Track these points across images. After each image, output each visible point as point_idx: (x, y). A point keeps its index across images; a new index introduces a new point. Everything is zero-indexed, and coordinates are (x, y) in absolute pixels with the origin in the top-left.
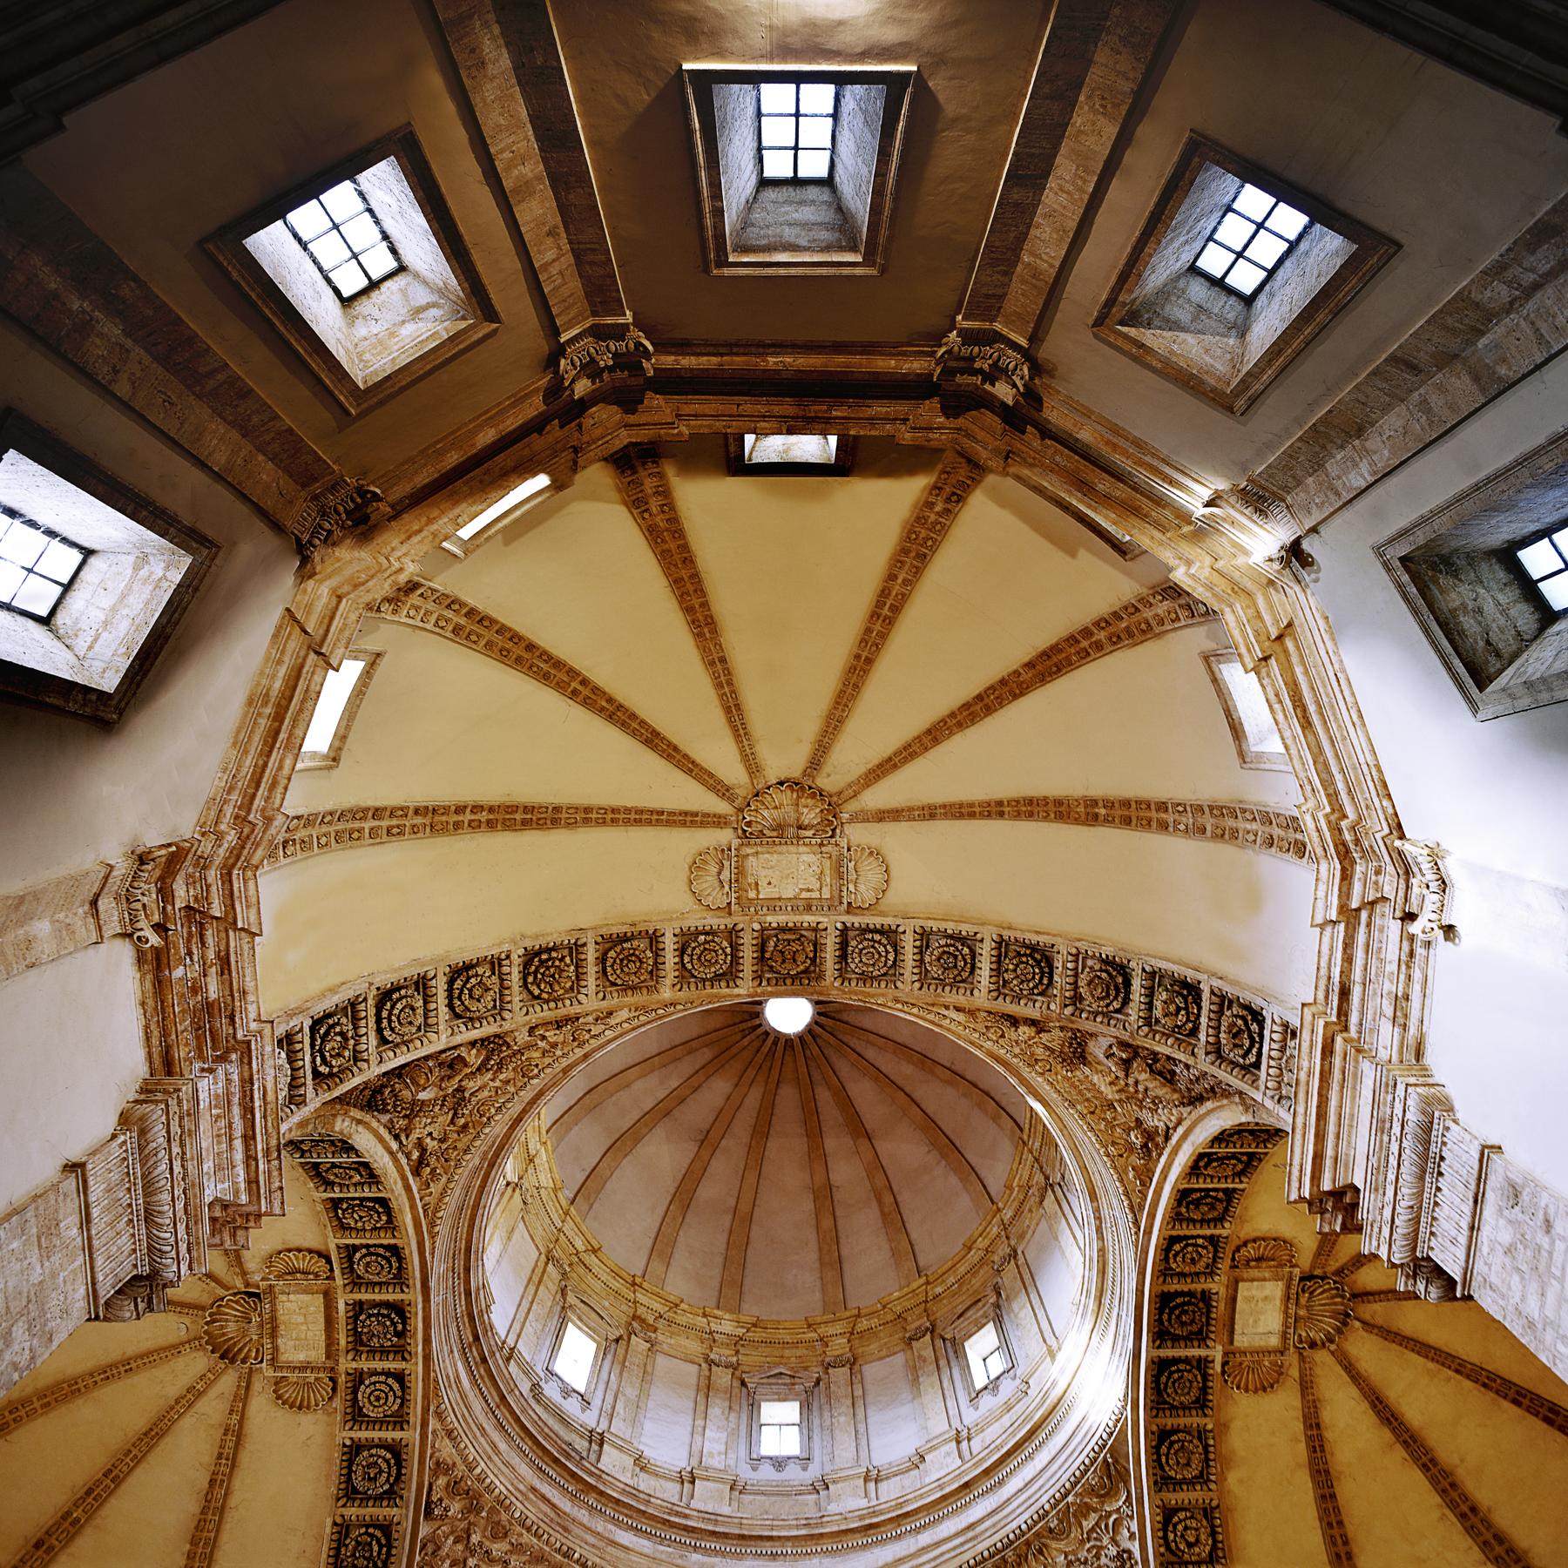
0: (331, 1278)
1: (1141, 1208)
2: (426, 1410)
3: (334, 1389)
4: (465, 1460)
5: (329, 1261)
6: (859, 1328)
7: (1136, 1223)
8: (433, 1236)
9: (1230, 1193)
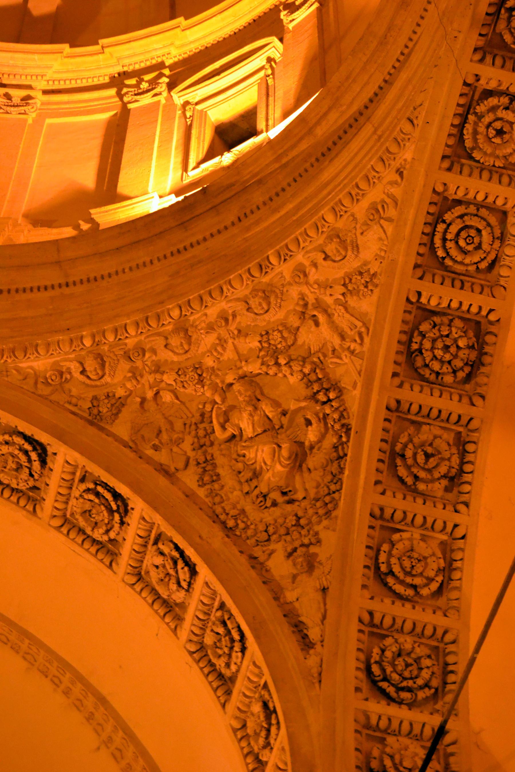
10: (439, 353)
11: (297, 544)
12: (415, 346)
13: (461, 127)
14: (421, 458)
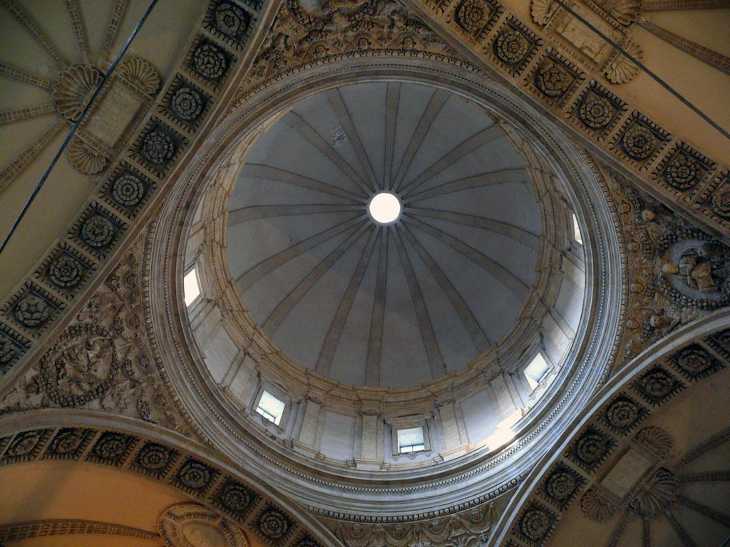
0: (154, 96)
1: (617, 370)
3: (105, 168)
4: (145, 266)
5: (161, 84)
6: (332, 393)
7: (607, 378)
9: (677, 385)
10: (110, 446)
11: (40, 385)
14: (68, 441)
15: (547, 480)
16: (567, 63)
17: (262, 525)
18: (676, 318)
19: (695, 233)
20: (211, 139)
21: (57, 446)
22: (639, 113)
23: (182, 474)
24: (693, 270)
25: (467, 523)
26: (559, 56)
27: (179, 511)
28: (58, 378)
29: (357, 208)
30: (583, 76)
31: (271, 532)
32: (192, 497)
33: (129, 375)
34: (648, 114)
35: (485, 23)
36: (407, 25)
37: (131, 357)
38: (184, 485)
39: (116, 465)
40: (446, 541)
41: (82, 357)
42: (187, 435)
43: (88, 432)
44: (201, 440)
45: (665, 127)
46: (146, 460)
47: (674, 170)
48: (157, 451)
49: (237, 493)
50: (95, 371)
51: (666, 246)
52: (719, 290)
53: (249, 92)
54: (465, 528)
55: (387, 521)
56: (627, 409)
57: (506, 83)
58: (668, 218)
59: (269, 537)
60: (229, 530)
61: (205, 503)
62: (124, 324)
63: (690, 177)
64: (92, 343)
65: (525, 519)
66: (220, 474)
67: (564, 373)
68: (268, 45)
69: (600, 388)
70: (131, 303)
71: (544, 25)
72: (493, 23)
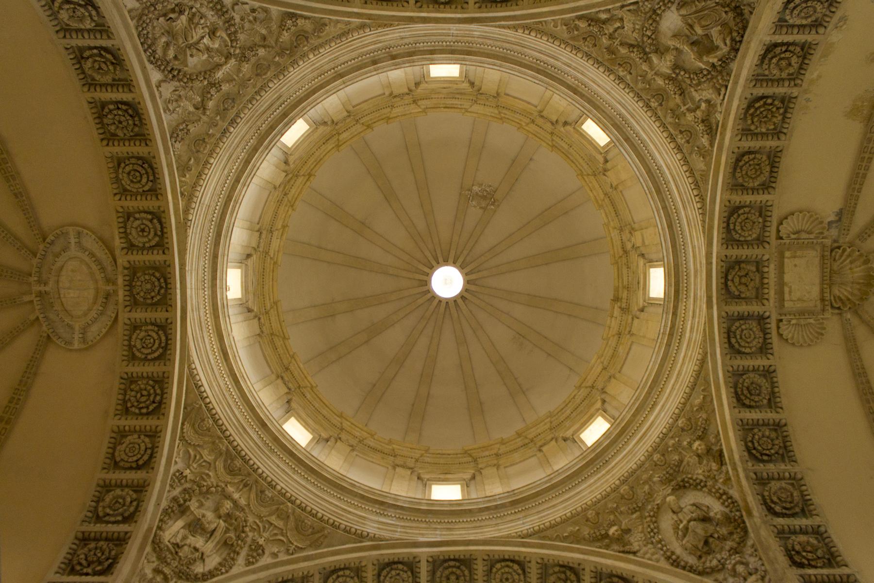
1: (544, 538)
2: (369, 17)
4: (321, 46)
7: (529, 536)
8: (515, 28)
10: (122, 119)
12: (136, 119)
13: (162, 228)
14: (103, 66)
15: (391, 564)
16: (766, 281)
17: (138, 332)
18: (635, 547)
19: (723, 496)
20: (477, 30)
21: (91, 56)
22: (774, 371)
23: (137, 216)
24: (695, 520)
25: (292, 523)
26: (766, 269)
27: (89, 242)
28: (165, 15)
29: (430, 258)
30: (765, 302)
31: (139, 345)
32: (118, 243)
33: (205, 94)
34: (780, 378)
35: (751, 185)
36: (703, 121)
37: (225, 87)
38: (125, 227)
39: (102, 140)
40: (260, 518)
41: (200, 32)
42: (182, 194)
43: (128, 84)
44: (187, 211)
45: (784, 401)
46: (128, 169)
47: (760, 434)
48: (147, 173)
49: (156, 283)
50: (192, 56)
51: (687, 485)
52: (700, 557)
53: (546, 34)
54: (286, 524)
55: (235, 448)
56: (516, 577)
57: (709, 244)
58: (714, 464)
59: (130, 347)
60: (105, 305)
61: (120, 261)
62: (253, 60)
63: (767, 452)
64: (218, 34)
65: (341, 573)
66: (164, 253)
67: (489, 501)
68: (604, 16)
69: (513, 537)
70: (279, 55)
71: (781, 238)
72: (755, 193)
